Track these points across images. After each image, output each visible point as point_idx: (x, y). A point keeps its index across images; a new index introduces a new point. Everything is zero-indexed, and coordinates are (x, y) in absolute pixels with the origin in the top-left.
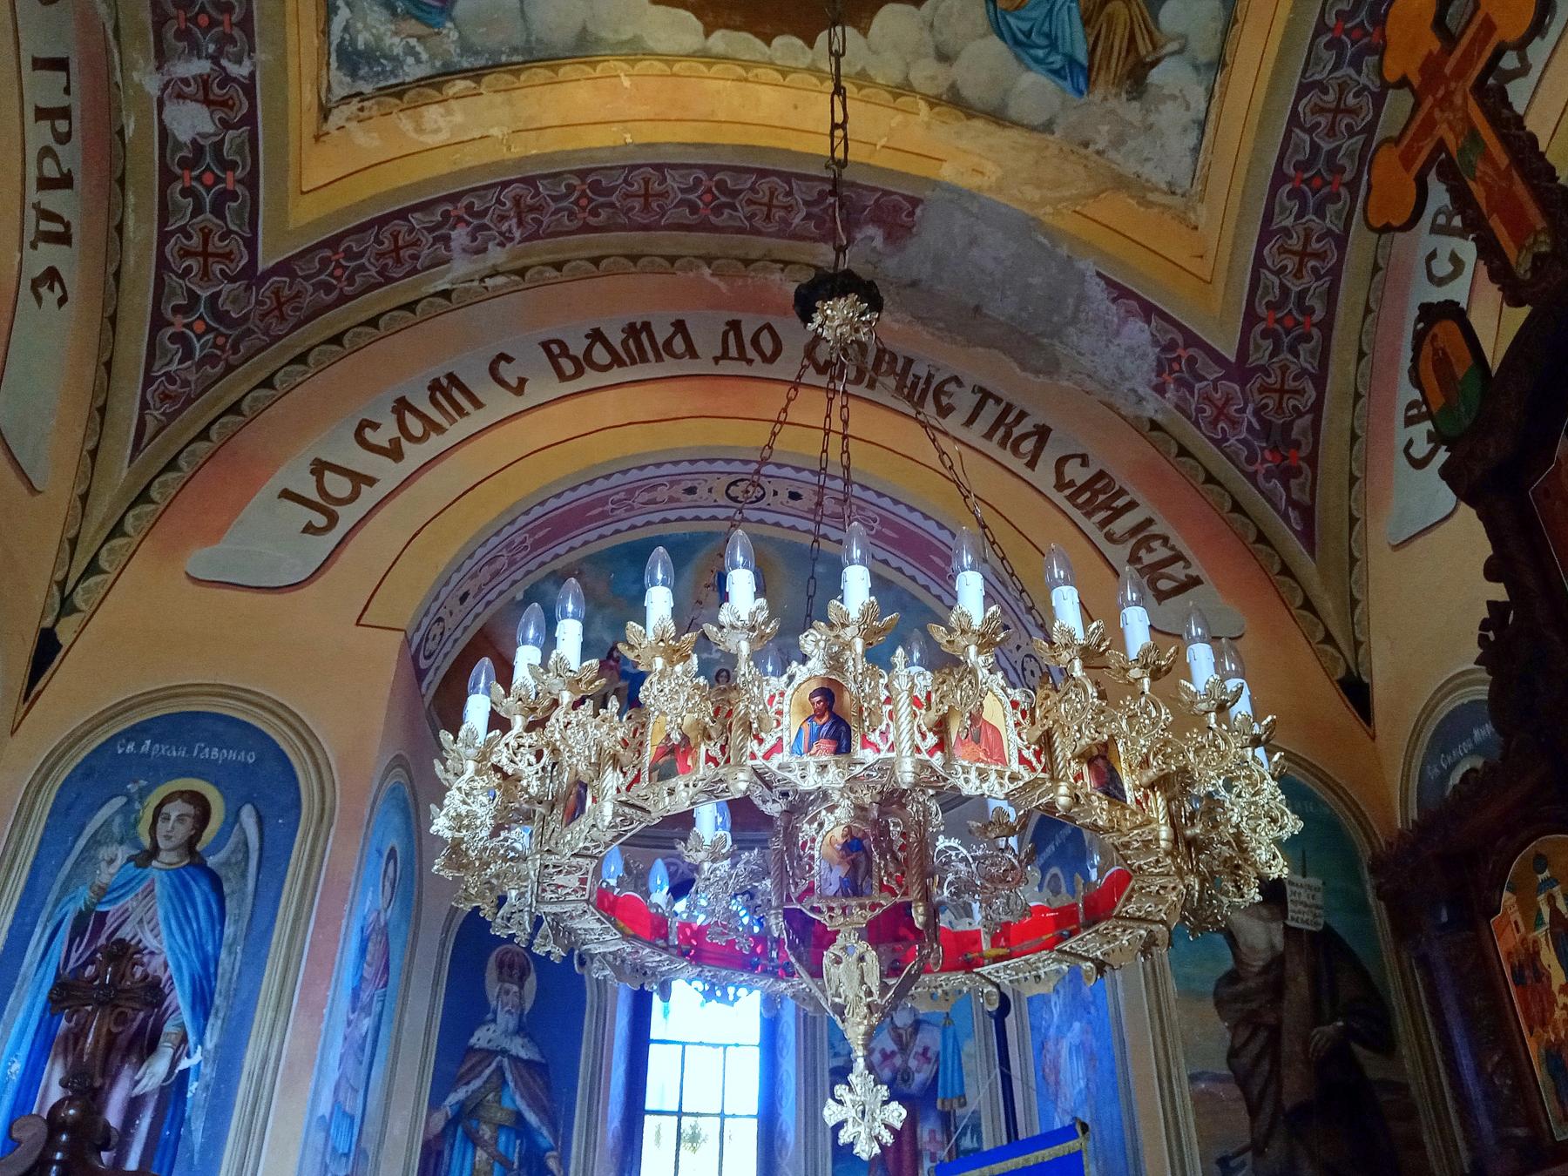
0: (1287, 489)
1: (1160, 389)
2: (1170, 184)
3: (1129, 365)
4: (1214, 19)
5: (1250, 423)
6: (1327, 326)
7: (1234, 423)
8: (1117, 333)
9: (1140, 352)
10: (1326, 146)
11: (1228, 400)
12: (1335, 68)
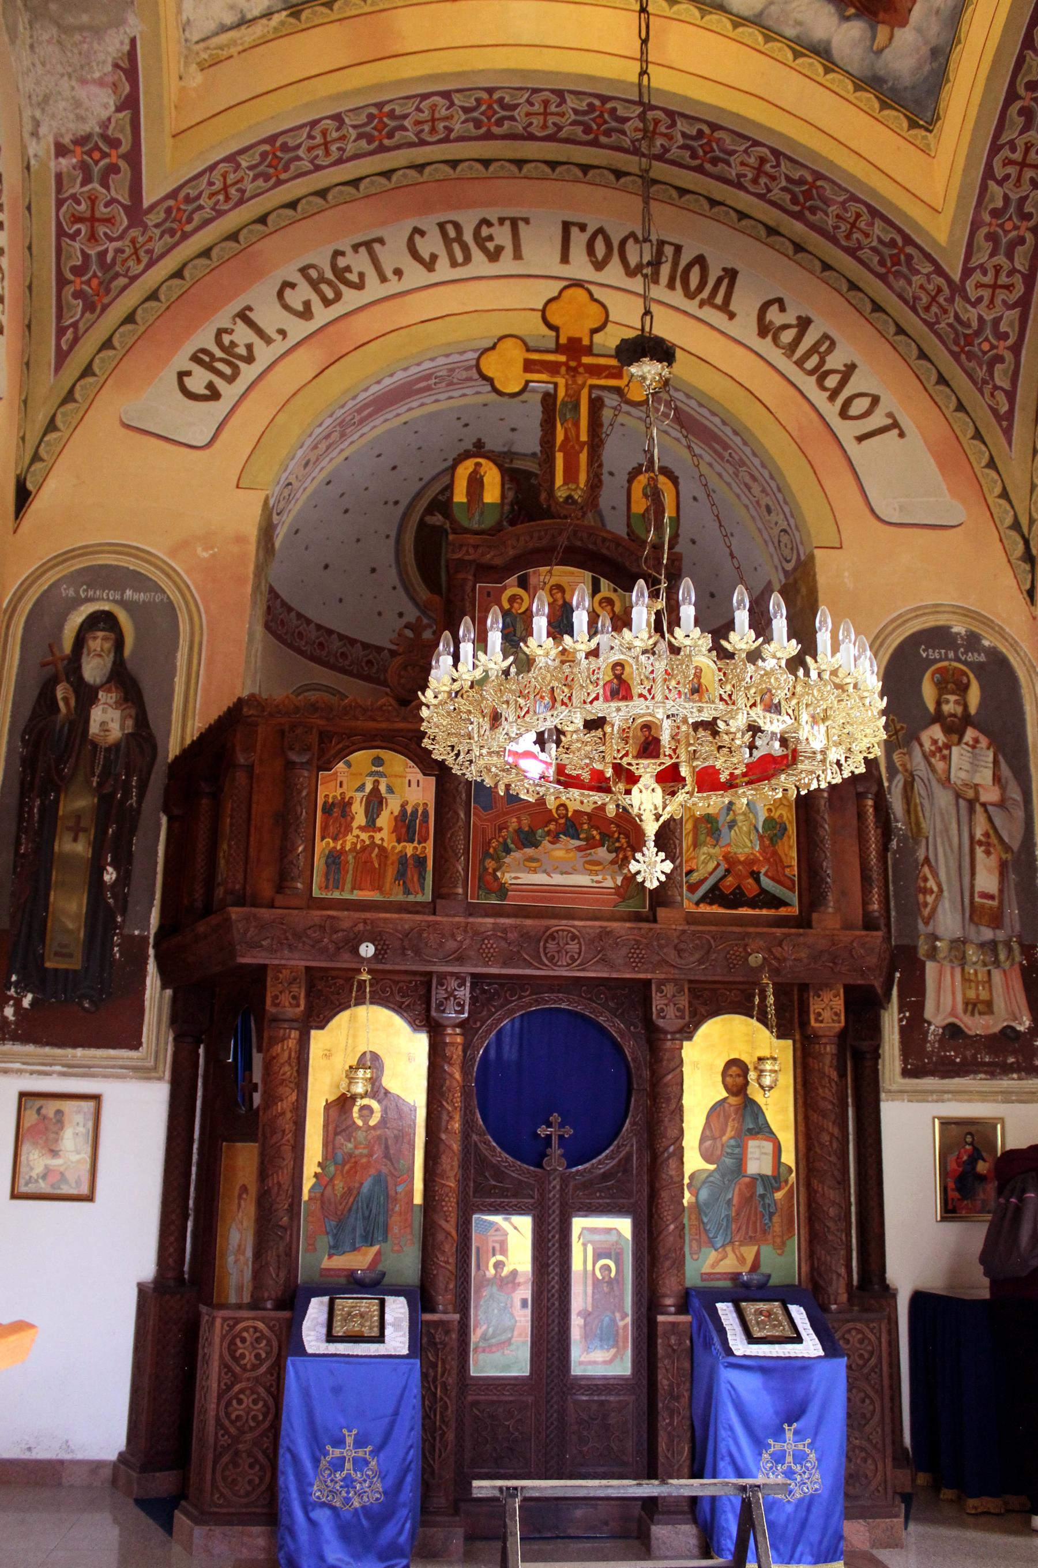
0: (82, 316)
1: (61, 150)
2: (188, 21)
3: (61, 106)
5: (106, 251)
6: (186, 236)
7: (93, 237)
8: (83, 82)
9: (82, 112)
10: (301, 153)
11: (109, 221)
12: (355, 127)
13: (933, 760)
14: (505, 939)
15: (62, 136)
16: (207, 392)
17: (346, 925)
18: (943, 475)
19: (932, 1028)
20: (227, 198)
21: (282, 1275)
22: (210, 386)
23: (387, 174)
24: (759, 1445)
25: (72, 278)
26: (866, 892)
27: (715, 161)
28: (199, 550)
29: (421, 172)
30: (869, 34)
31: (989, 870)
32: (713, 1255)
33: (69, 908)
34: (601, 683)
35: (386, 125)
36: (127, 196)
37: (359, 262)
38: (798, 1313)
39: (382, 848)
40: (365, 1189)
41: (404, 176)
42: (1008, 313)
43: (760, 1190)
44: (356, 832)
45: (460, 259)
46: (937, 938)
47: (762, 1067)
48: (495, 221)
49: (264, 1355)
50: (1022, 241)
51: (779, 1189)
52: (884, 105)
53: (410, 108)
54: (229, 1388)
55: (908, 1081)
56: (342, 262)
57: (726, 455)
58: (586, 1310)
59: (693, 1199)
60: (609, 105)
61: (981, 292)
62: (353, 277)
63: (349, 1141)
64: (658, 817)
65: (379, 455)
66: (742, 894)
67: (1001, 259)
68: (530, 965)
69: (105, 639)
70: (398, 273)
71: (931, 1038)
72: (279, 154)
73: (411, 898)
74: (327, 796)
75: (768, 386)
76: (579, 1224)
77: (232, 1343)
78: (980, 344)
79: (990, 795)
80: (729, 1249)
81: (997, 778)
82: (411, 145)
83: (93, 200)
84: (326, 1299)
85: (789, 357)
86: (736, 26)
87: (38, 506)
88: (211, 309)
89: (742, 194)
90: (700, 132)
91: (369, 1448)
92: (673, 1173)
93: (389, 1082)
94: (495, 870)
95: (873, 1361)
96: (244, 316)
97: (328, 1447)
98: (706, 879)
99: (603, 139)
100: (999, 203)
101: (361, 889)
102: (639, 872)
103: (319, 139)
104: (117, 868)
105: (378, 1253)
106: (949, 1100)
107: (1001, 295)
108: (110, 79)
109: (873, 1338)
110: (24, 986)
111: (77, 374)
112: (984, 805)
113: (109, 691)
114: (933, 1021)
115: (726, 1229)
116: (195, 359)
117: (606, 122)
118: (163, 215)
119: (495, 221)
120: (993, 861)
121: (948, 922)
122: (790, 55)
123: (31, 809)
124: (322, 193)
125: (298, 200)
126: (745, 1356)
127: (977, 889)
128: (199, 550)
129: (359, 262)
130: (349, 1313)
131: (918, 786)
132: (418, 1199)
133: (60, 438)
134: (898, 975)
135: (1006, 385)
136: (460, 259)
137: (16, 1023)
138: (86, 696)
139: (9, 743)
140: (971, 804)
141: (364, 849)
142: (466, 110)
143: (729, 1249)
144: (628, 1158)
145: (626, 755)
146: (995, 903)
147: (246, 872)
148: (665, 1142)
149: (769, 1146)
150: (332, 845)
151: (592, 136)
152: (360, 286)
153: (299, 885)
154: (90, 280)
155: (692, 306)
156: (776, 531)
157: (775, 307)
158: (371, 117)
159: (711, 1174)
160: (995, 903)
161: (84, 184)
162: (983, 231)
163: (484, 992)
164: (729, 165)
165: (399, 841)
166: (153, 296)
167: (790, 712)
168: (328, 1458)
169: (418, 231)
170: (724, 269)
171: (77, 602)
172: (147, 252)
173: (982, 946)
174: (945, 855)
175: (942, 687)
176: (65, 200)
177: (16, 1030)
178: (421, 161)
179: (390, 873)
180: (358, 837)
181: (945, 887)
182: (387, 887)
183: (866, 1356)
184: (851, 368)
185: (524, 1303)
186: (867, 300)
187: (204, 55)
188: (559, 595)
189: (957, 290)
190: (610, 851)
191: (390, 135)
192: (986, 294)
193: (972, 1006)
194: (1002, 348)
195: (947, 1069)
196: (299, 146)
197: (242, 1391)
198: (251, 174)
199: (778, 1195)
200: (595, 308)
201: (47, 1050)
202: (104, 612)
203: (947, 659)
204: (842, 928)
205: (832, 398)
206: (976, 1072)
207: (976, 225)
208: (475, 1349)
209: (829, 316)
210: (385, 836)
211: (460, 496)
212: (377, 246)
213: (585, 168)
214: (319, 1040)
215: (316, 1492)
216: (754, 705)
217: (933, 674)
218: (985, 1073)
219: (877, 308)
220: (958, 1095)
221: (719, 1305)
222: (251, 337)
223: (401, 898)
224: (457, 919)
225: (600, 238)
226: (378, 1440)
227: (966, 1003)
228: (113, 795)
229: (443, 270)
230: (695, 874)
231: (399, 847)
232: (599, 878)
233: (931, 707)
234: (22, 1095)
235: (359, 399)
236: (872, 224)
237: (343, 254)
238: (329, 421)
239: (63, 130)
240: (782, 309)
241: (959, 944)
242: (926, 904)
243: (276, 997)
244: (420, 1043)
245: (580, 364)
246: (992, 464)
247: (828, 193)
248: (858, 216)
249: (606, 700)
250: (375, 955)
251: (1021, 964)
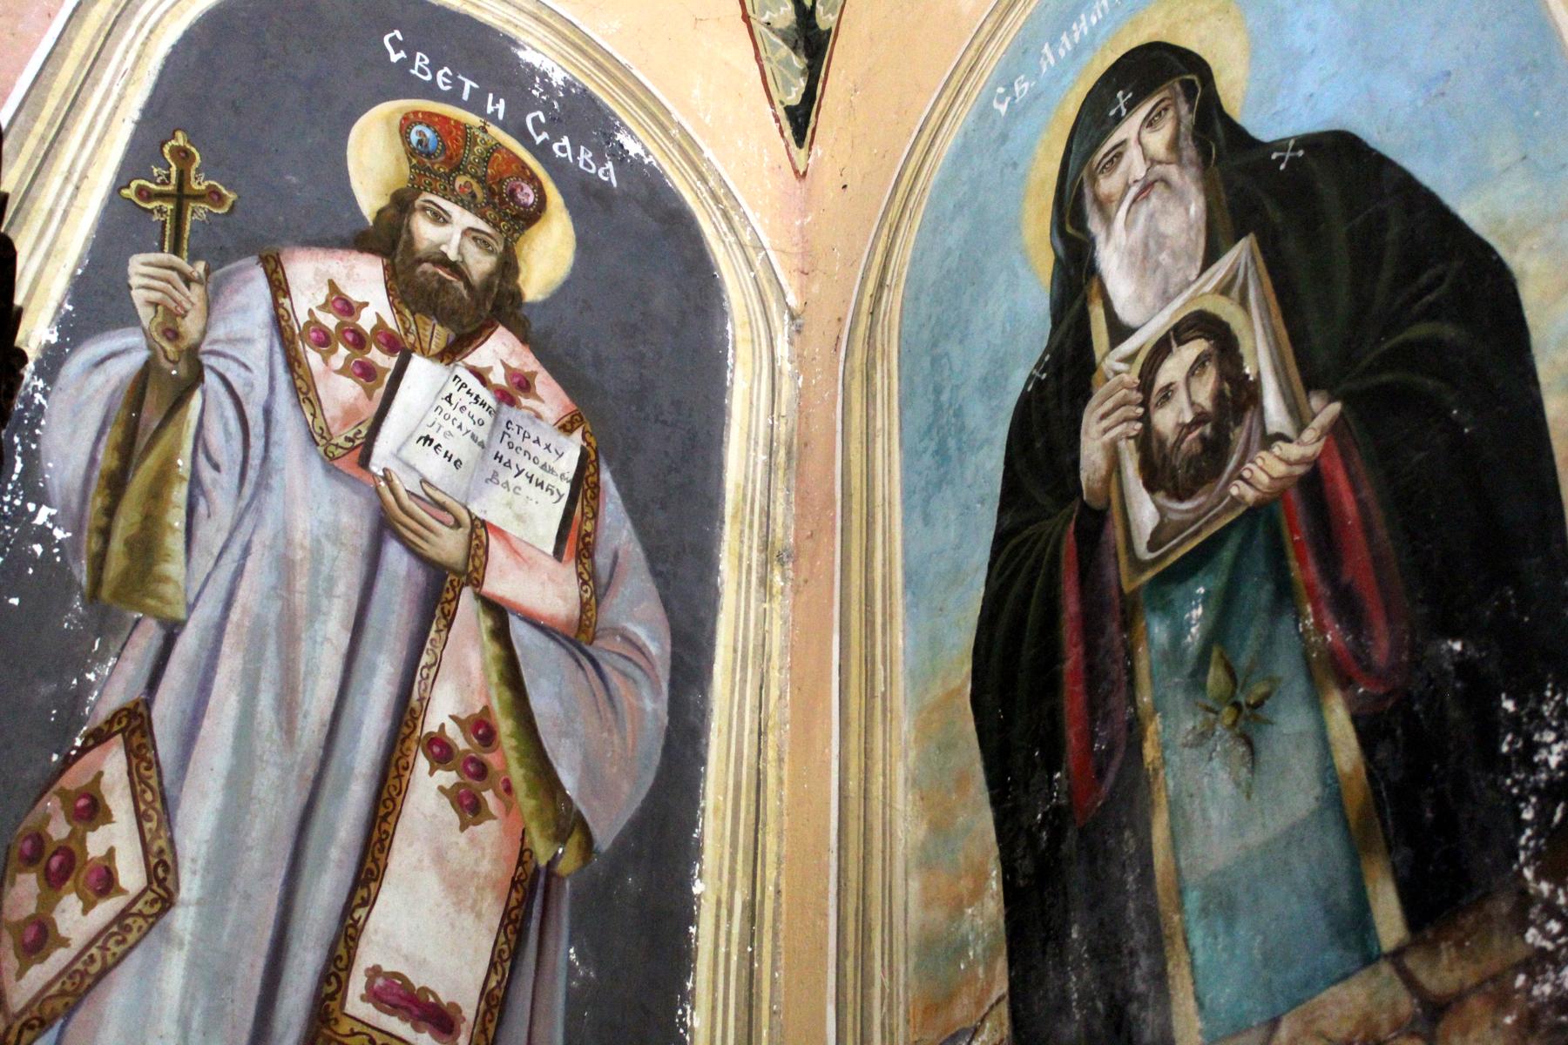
13: (313, 358)
31: (455, 884)
79: (538, 585)
81: (575, 539)
112: (498, 611)
120: (486, 849)
127: (370, 954)
140: (440, 588)
175: (438, 162)
181: (190, 886)
203: (476, 105)
233: (370, 199)
242: (38, 938)
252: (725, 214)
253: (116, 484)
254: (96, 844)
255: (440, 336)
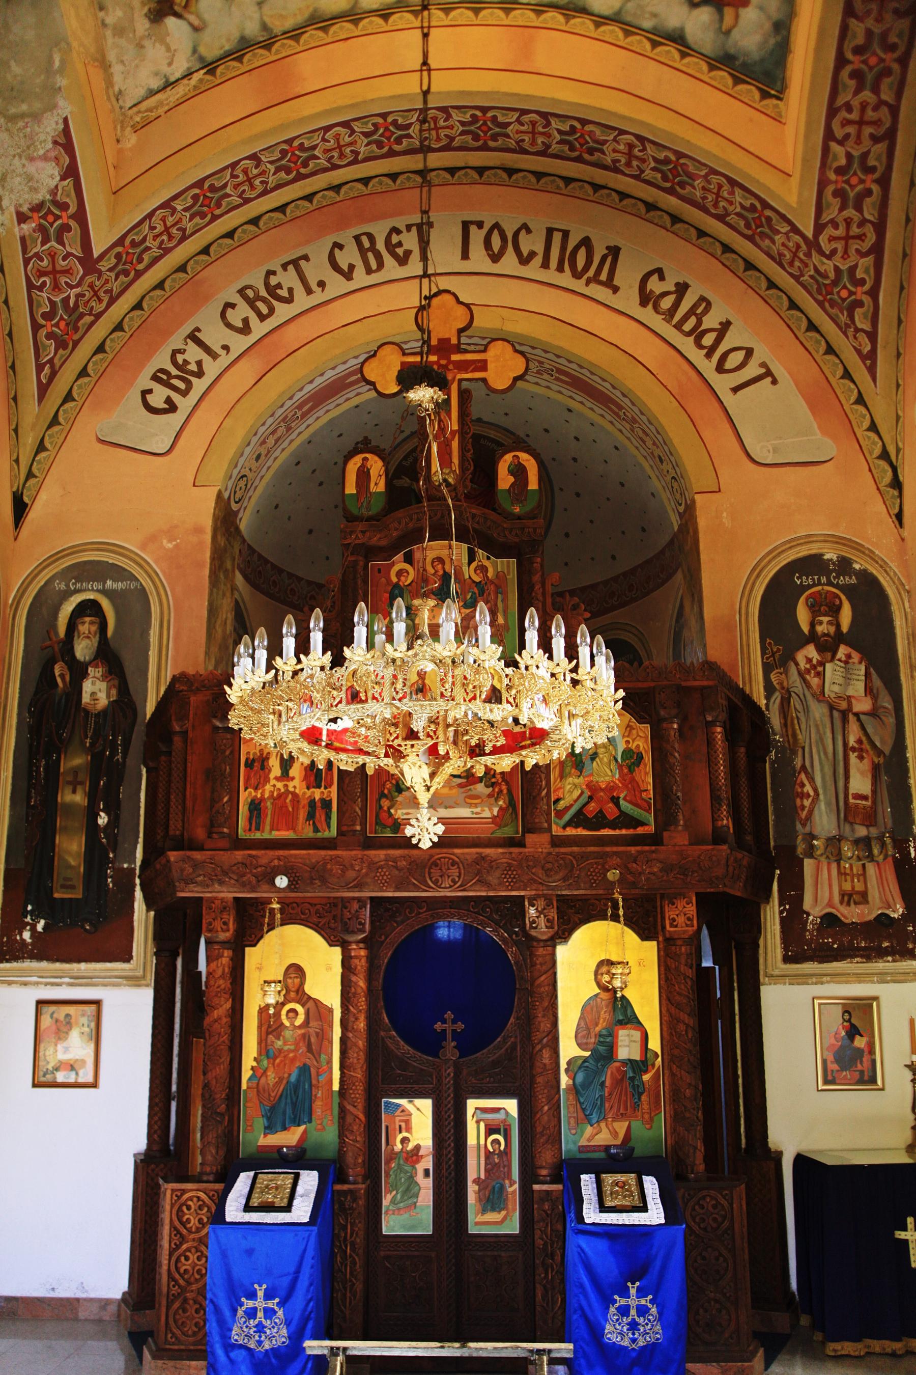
1: (22, 218)
2: (120, 92)
3: (16, 182)
4: (228, 40)
5: (69, 297)
6: (139, 274)
7: (56, 287)
8: (32, 159)
9: (35, 185)
10: (228, 190)
11: (67, 272)
12: (271, 162)
13: (808, 677)
14: (396, 868)
15: (21, 205)
16: (166, 406)
17: (264, 861)
18: (813, 413)
19: (811, 918)
20: (170, 238)
21: (222, 1153)
22: (169, 400)
23: (309, 198)
24: (608, 1301)
25: (44, 322)
26: (715, 810)
27: (591, 151)
28: (165, 542)
29: (338, 193)
30: (716, 17)
31: (862, 773)
32: (589, 1130)
33: (71, 848)
34: (344, 689)
35: (300, 157)
36: (79, 249)
37: (288, 279)
38: (651, 1185)
39: (295, 795)
40: (293, 1078)
41: (324, 197)
42: (862, 261)
43: (630, 1074)
44: (273, 782)
45: (374, 267)
46: (814, 837)
47: (614, 971)
48: (403, 229)
49: (205, 1220)
50: (869, 192)
51: (646, 1072)
52: (737, 81)
53: (316, 139)
54: (178, 1247)
55: (788, 966)
56: (273, 281)
57: (621, 414)
58: (479, 1178)
59: (571, 1082)
60: (490, 114)
61: (834, 245)
62: (284, 293)
63: (278, 1039)
64: (428, 788)
65: (340, 435)
66: (604, 817)
67: (850, 212)
68: (418, 889)
69: (91, 623)
70: (322, 284)
71: (810, 927)
72: (208, 194)
73: (319, 835)
74: (248, 753)
75: (649, 351)
76: (472, 1104)
77: (180, 1210)
78: (838, 293)
80: (603, 1125)
81: (869, 690)
82: (325, 170)
83: (52, 256)
84: (252, 1173)
85: (668, 322)
86: (598, 25)
87: (33, 515)
88: (167, 334)
89: (620, 176)
90: (572, 127)
91: (277, 1300)
92: (546, 1061)
93: (312, 988)
94: (389, 809)
95: (726, 1224)
96: (193, 337)
97: (243, 1299)
98: (572, 805)
99: (491, 144)
100: (843, 162)
101: (278, 830)
102: (413, 836)
103: (242, 177)
104: (107, 813)
105: (305, 1132)
106: (828, 982)
107: (854, 245)
108: (52, 154)
109: (725, 1203)
110: (36, 915)
111: (60, 402)
112: (857, 715)
113: (96, 666)
114: (812, 912)
115: (600, 1108)
116: (155, 378)
117: (491, 129)
118: (114, 261)
119: (403, 229)
120: (866, 765)
121: (824, 822)
122: (648, 46)
123: (38, 768)
124: (255, 221)
125: (236, 229)
126: (594, 1224)
128: (165, 542)
129: (288, 279)
130: (267, 1187)
131: (795, 702)
132: (336, 1087)
133: (49, 456)
134: (778, 872)
135: (867, 327)
136: (374, 267)
137: (31, 944)
138: (79, 672)
139: (19, 714)
140: (844, 715)
141: (280, 796)
142: (366, 135)
143: (603, 1125)
144: (513, 1047)
145: (397, 738)
146: (868, 803)
147: (183, 821)
148: (539, 1035)
149: (637, 1035)
150: (253, 794)
151: (481, 142)
152: (289, 300)
153: (225, 830)
154: (58, 323)
155: (578, 285)
156: (669, 478)
157: (656, 276)
158: (284, 153)
159: (586, 1060)
160: (869, 803)
161: (43, 244)
162: (831, 188)
163: (387, 910)
164: (603, 153)
165: (308, 788)
166: (119, 327)
167: (511, 700)
168: (244, 1308)
169: (338, 246)
170: (607, 248)
171: (67, 594)
172: (105, 292)
173: (857, 842)
174: (821, 763)
175: (815, 609)
176: (31, 258)
177: (32, 950)
178: (336, 182)
179: (302, 814)
180: (274, 786)
181: (821, 791)
182: (300, 827)
183: (720, 1219)
184: (726, 326)
185: (427, 1172)
186: (740, 261)
187: (138, 119)
188: (440, 566)
189: (813, 245)
190: (487, 786)
191: (305, 164)
192: (840, 246)
193: (847, 897)
194: (860, 293)
195: (825, 955)
196: (225, 186)
197: (188, 1250)
198: (188, 215)
199: (646, 1077)
200: (461, 310)
201: (58, 965)
202: (89, 600)
203: (820, 584)
204: (691, 844)
205: (709, 355)
206: (852, 957)
207: (822, 184)
208: (386, 1213)
209: (706, 280)
210: (297, 784)
211: (351, 489)
212: (303, 263)
213: (481, 170)
214: (252, 955)
215: (236, 1335)
216: (474, 698)
217: (807, 600)
218: (862, 957)
219: (750, 266)
220: (835, 977)
221: (583, 1177)
222: (201, 355)
223: (311, 835)
224: (354, 852)
225: (496, 232)
226: (283, 1293)
227: (843, 894)
228: (104, 751)
229: (361, 278)
230: (562, 802)
231: (309, 793)
232: (478, 810)
233: (805, 628)
234: (40, 1003)
235: (296, 398)
236: (732, 193)
237: (274, 273)
238: (270, 421)
239: (21, 201)
240: (662, 278)
241: (834, 842)
243: (210, 924)
244: (337, 952)
245: (450, 362)
246: (860, 400)
247: (691, 169)
248: (720, 186)
249: (348, 703)
250: (288, 886)
251: (894, 856)
252: (886, 571)
253: (785, 725)
254: (805, 790)
255: (829, 655)
